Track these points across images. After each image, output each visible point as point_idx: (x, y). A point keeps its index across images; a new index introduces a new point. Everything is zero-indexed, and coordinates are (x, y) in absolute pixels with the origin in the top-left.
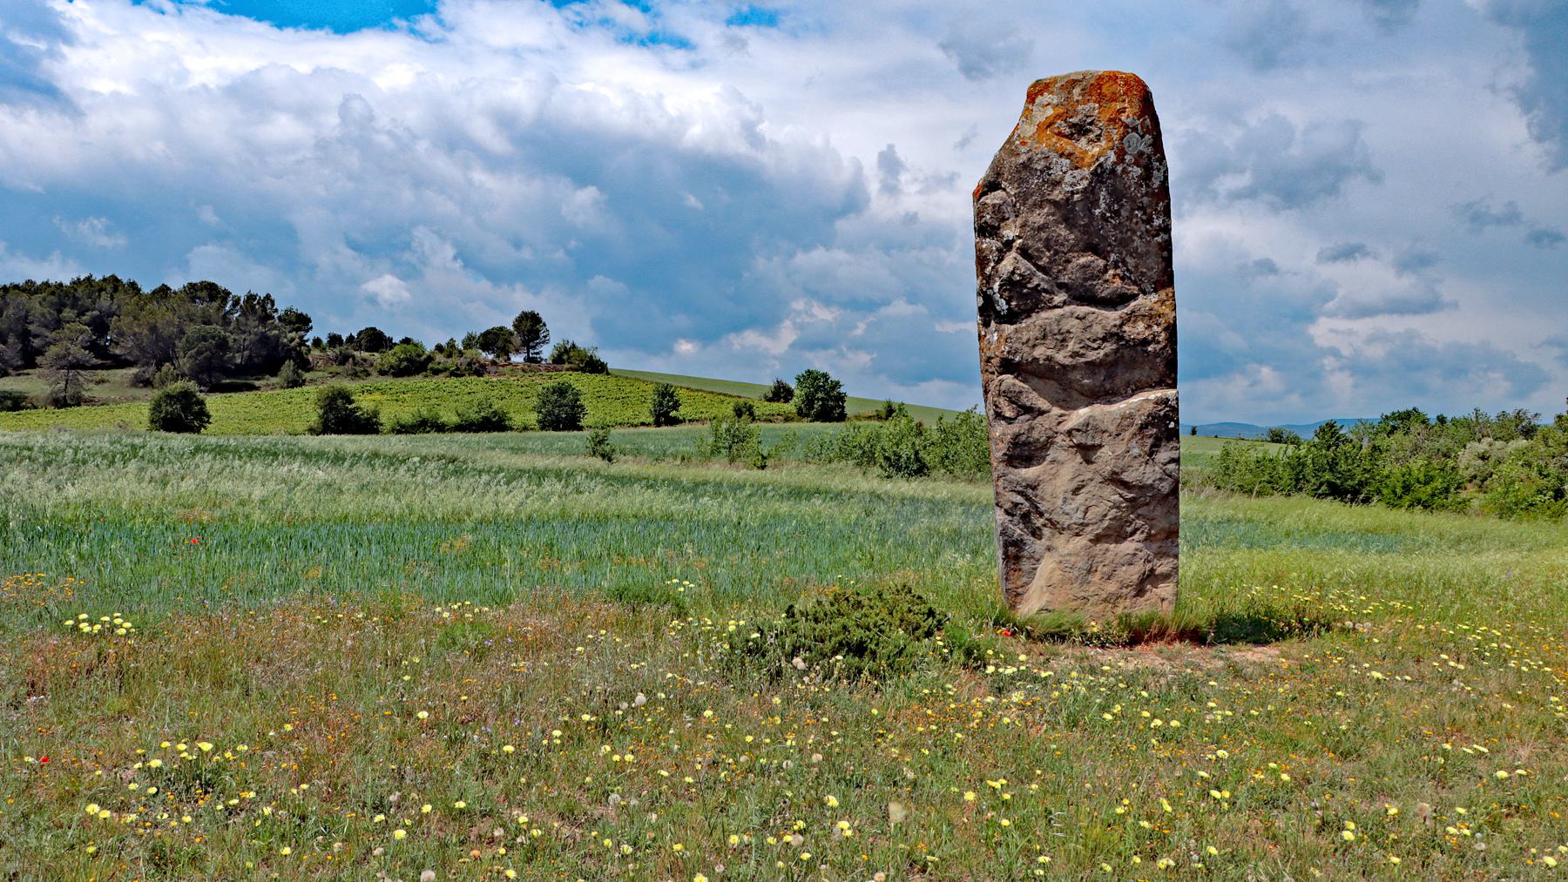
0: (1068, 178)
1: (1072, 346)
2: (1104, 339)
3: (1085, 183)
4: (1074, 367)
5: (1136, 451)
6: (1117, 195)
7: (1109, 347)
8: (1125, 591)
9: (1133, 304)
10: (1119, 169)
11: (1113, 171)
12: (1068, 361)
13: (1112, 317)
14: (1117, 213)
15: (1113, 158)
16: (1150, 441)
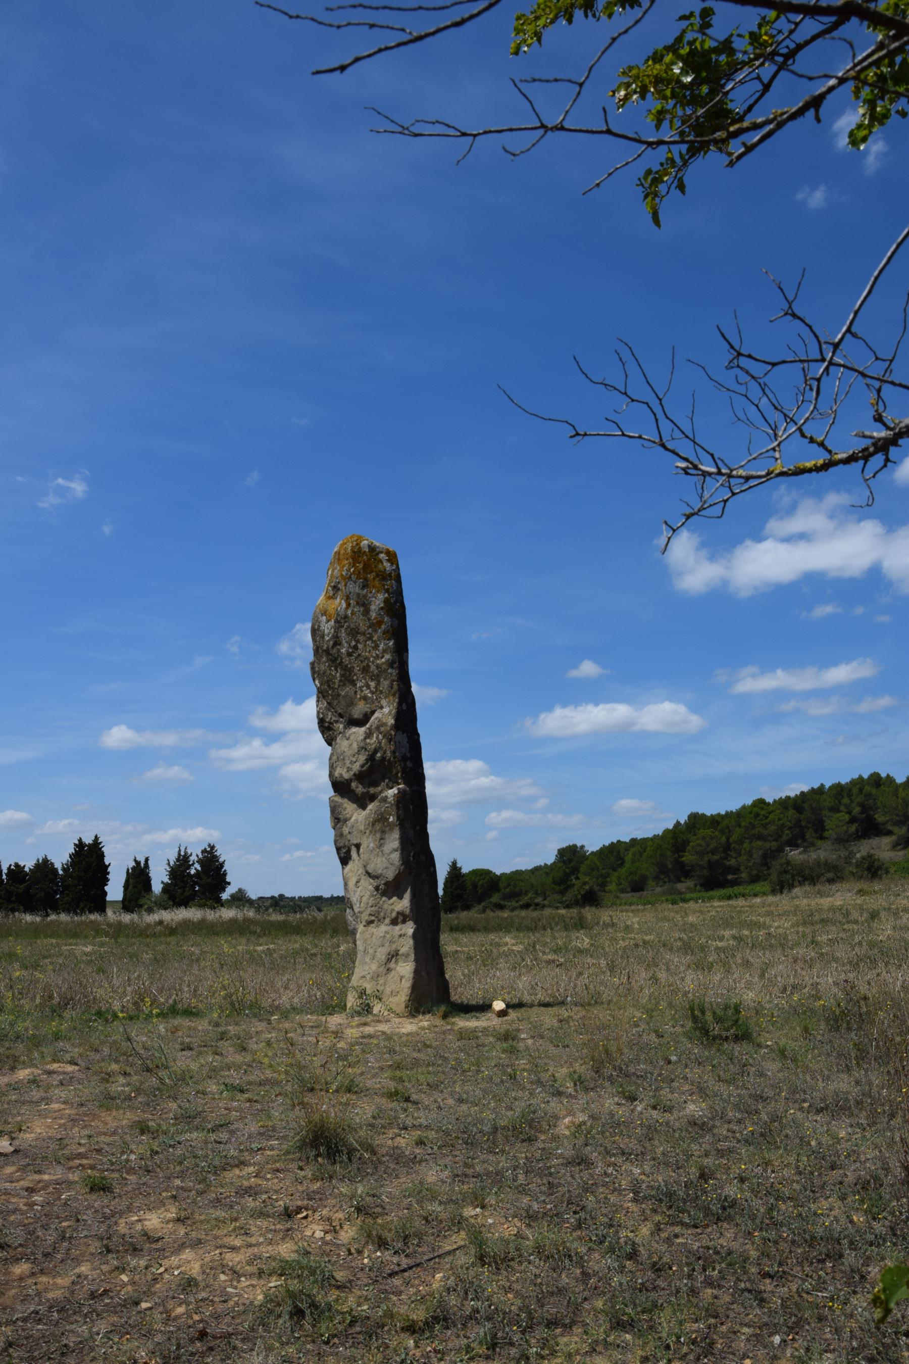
0: (326, 631)
1: (348, 762)
2: (358, 753)
3: (332, 631)
4: (350, 780)
5: (372, 845)
6: (354, 633)
7: (362, 758)
8: (381, 969)
9: (373, 718)
10: (349, 612)
11: (346, 617)
12: (346, 776)
13: (360, 731)
14: (356, 648)
15: (344, 605)
16: (378, 835)
